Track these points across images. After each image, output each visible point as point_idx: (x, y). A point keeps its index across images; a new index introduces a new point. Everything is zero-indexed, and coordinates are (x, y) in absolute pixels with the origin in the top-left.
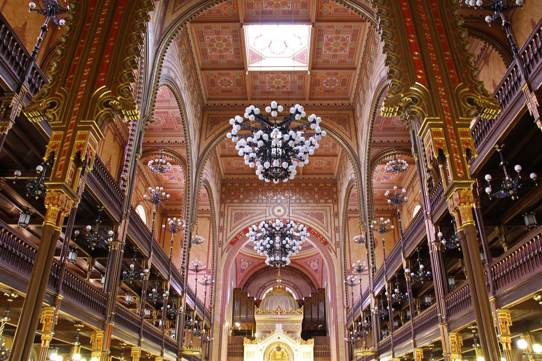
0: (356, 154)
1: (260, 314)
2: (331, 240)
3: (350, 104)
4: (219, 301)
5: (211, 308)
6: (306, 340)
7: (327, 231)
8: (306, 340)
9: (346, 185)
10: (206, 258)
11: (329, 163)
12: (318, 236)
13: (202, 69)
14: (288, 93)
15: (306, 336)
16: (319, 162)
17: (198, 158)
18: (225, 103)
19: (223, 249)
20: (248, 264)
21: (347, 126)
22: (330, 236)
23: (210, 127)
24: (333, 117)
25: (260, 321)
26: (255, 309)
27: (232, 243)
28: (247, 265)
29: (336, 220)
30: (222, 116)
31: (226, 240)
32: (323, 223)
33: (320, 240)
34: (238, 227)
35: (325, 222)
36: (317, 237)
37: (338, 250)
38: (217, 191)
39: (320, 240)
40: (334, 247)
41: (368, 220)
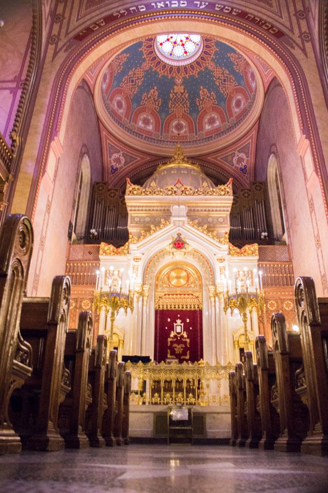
1: (137, 194)
2: (292, 30)
4: (36, 133)
6: (240, 247)
7: (281, 17)
8: (240, 247)
10: (18, 62)
12: (263, 24)
15: (238, 239)
19: (59, 47)
20: (122, 158)
22: (288, 24)
25: (138, 209)
26: (128, 185)
27: (79, 38)
28: (123, 162)
31: (67, 34)
32: (271, 5)
33: (268, 30)
34: (94, 14)
35: (274, 4)
36: (261, 26)
37: (308, 46)
39: (268, 30)
40: (299, 41)
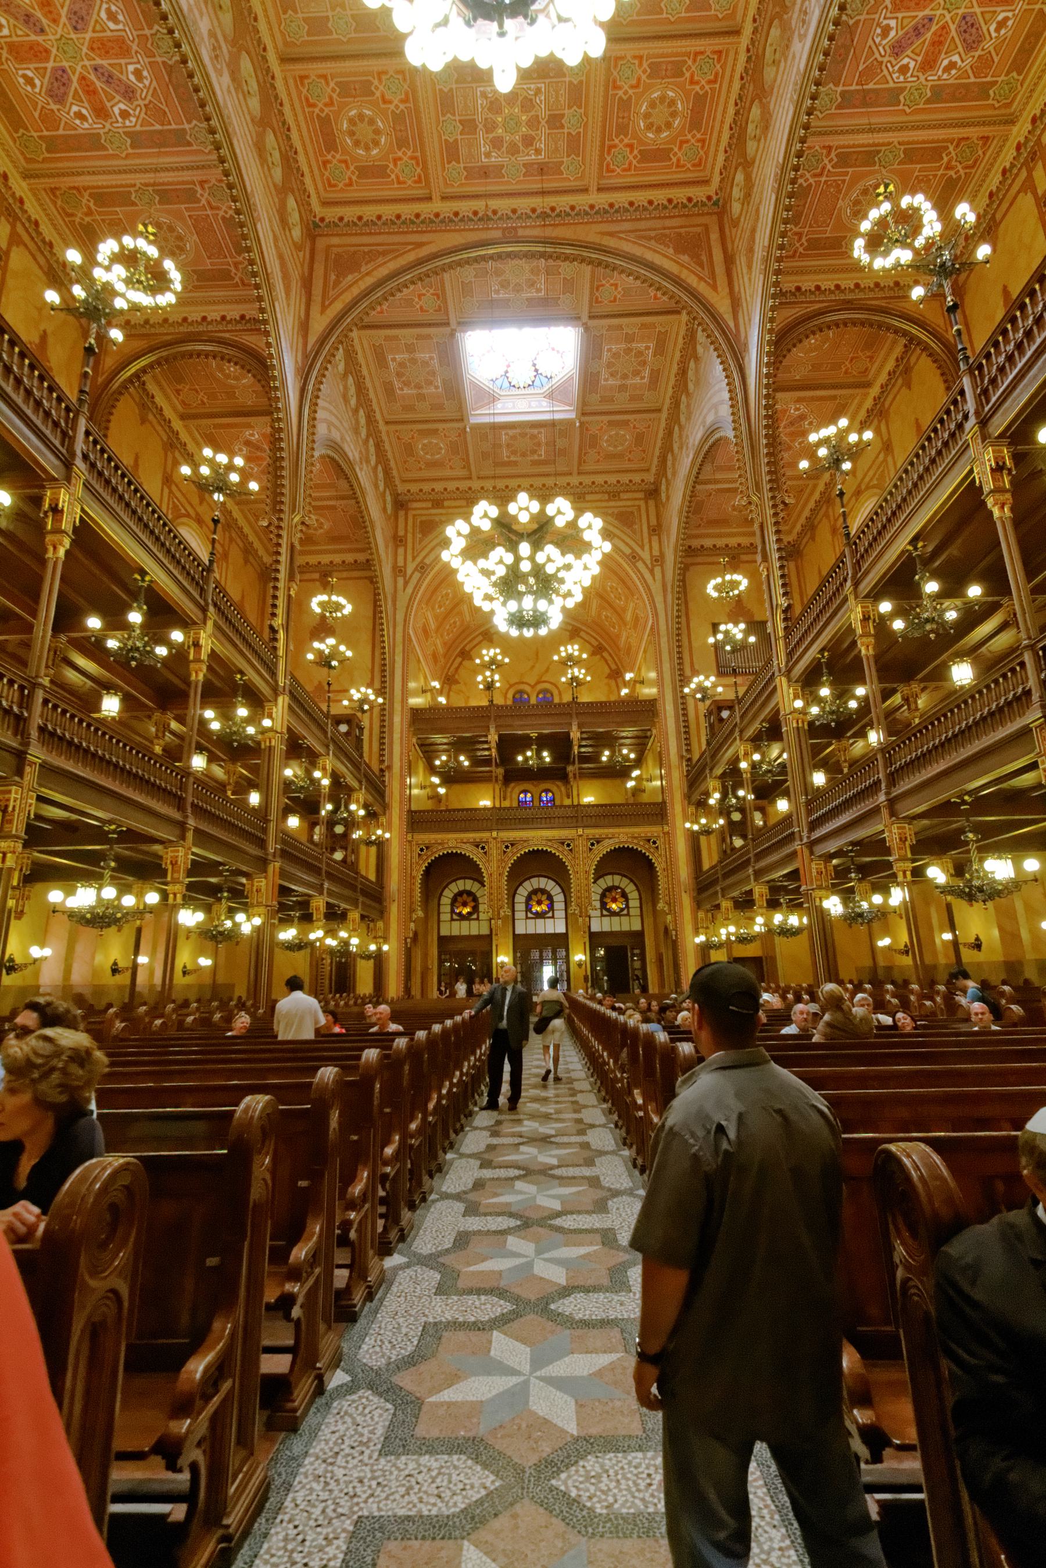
0: (728, 326)
3: (709, 198)
5: (382, 770)
9: (685, 463)
11: (639, 439)
13: (284, 60)
14: (542, 169)
16: (617, 434)
17: (305, 356)
18: (369, 212)
21: (704, 258)
23: (333, 277)
24: (665, 235)
29: (657, 570)
30: (366, 249)
38: (384, 509)
41: (766, 487)
